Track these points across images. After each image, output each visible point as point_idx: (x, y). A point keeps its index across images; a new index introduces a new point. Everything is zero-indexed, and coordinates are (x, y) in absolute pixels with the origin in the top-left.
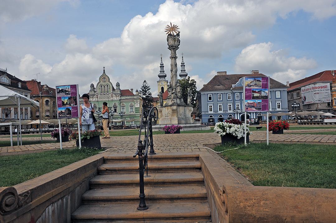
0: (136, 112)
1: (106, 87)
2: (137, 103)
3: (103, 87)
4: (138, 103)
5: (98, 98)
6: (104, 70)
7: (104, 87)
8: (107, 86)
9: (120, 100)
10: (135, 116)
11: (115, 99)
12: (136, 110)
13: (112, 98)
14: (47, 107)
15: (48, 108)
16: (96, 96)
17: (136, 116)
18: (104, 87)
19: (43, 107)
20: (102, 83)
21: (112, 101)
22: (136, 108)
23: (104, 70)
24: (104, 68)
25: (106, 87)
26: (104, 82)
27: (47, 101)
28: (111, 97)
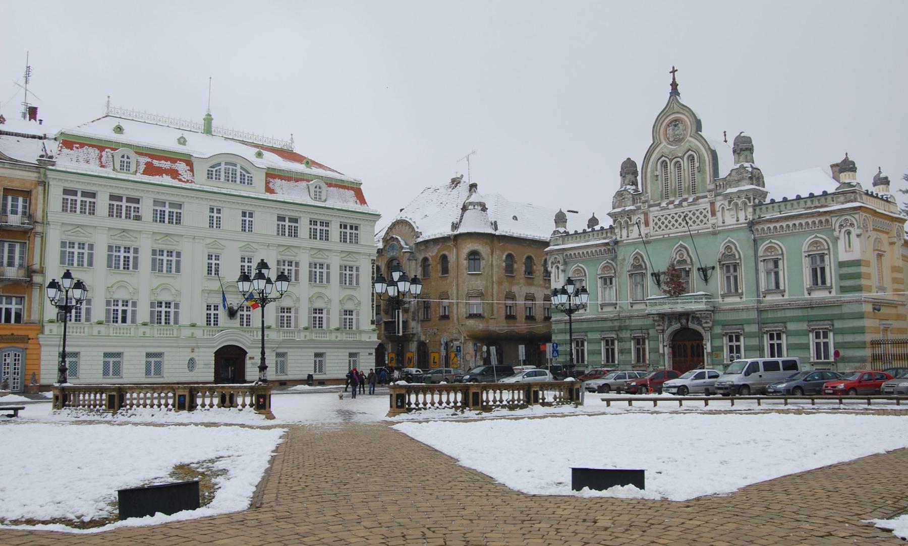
0: (843, 290)
1: (685, 163)
2: (849, 233)
3: (671, 166)
4: (854, 231)
5: (651, 224)
6: (674, 85)
7: (678, 166)
8: (691, 158)
9: (751, 224)
10: (836, 311)
11: (730, 220)
12: (842, 277)
13: (712, 220)
14: (473, 278)
15: (479, 284)
16: (642, 217)
17: (847, 309)
18: (678, 166)
19: (460, 280)
20: (665, 147)
21: (714, 234)
22: (842, 265)
23: (674, 85)
24: (674, 71)
25: (685, 163)
26: (678, 140)
27: (474, 256)
28: (709, 215)
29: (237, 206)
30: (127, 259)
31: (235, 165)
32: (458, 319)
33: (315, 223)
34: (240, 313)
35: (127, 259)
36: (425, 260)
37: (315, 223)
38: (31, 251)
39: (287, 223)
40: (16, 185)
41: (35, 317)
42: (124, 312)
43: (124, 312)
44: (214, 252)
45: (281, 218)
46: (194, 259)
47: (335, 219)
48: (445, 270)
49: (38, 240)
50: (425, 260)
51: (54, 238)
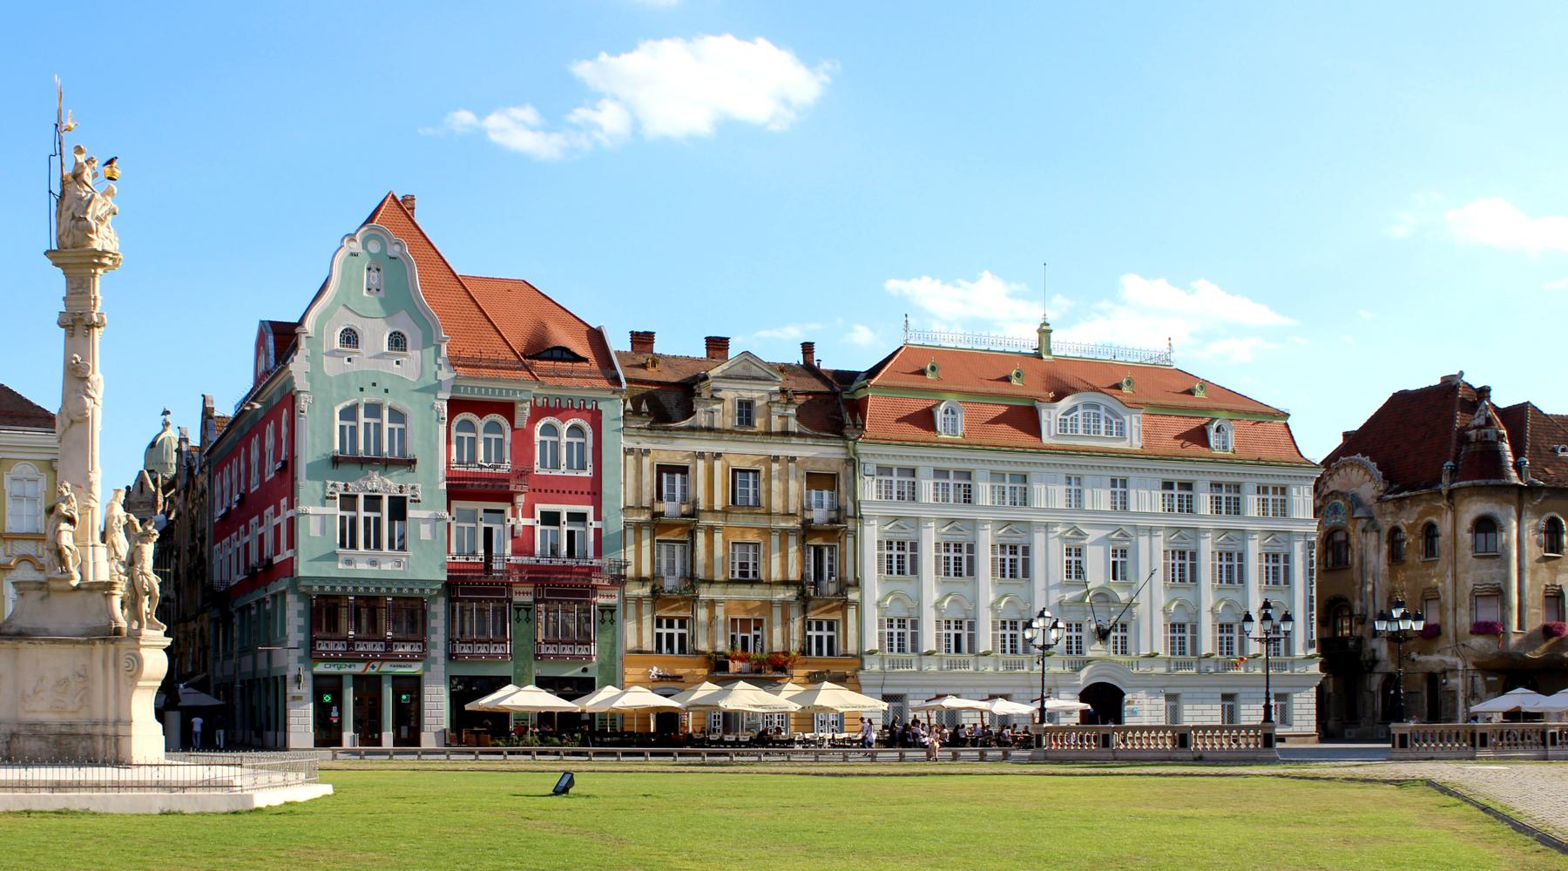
29: (1104, 472)
30: (958, 561)
31: (1098, 407)
32: (1456, 635)
33: (1265, 490)
34: (1113, 634)
35: (958, 561)
36: (1395, 530)
37: (1265, 490)
38: (843, 555)
39: (1176, 492)
40: (820, 468)
41: (852, 647)
42: (958, 637)
43: (958, 637)
44: (1074, 544)
45: (1168, 485)
46: (1048, 557)
47: (1201, 477)
48: (1430, 551)
49: (850, 541)
50: (1395, 530)
51: (871, 535)
